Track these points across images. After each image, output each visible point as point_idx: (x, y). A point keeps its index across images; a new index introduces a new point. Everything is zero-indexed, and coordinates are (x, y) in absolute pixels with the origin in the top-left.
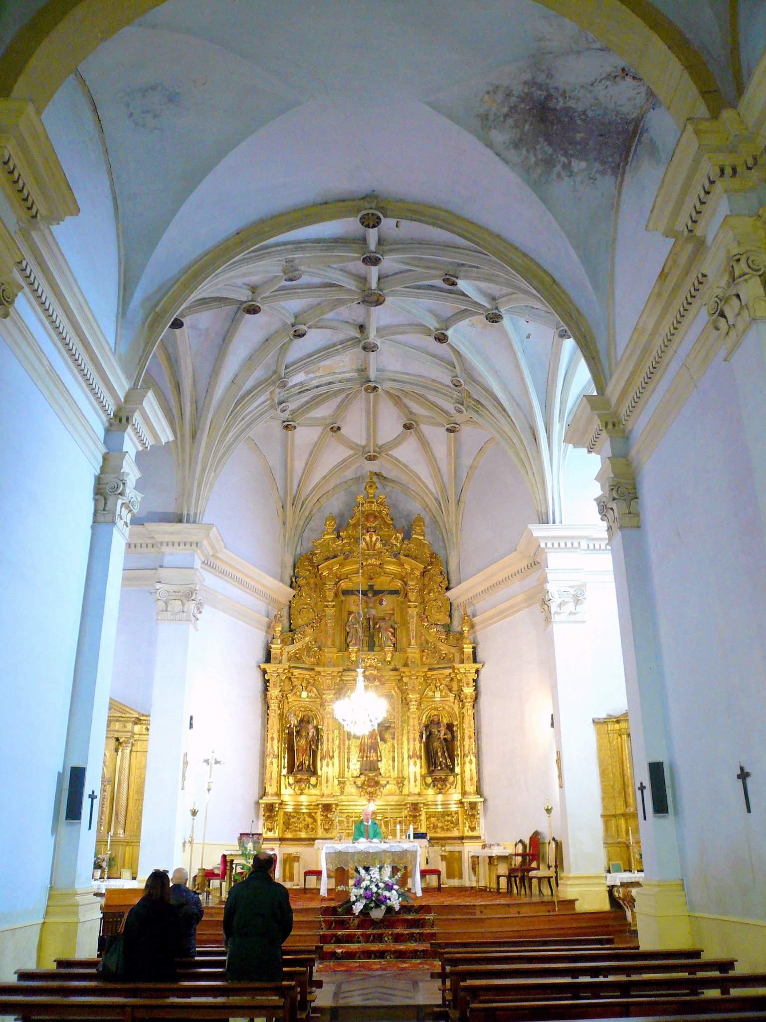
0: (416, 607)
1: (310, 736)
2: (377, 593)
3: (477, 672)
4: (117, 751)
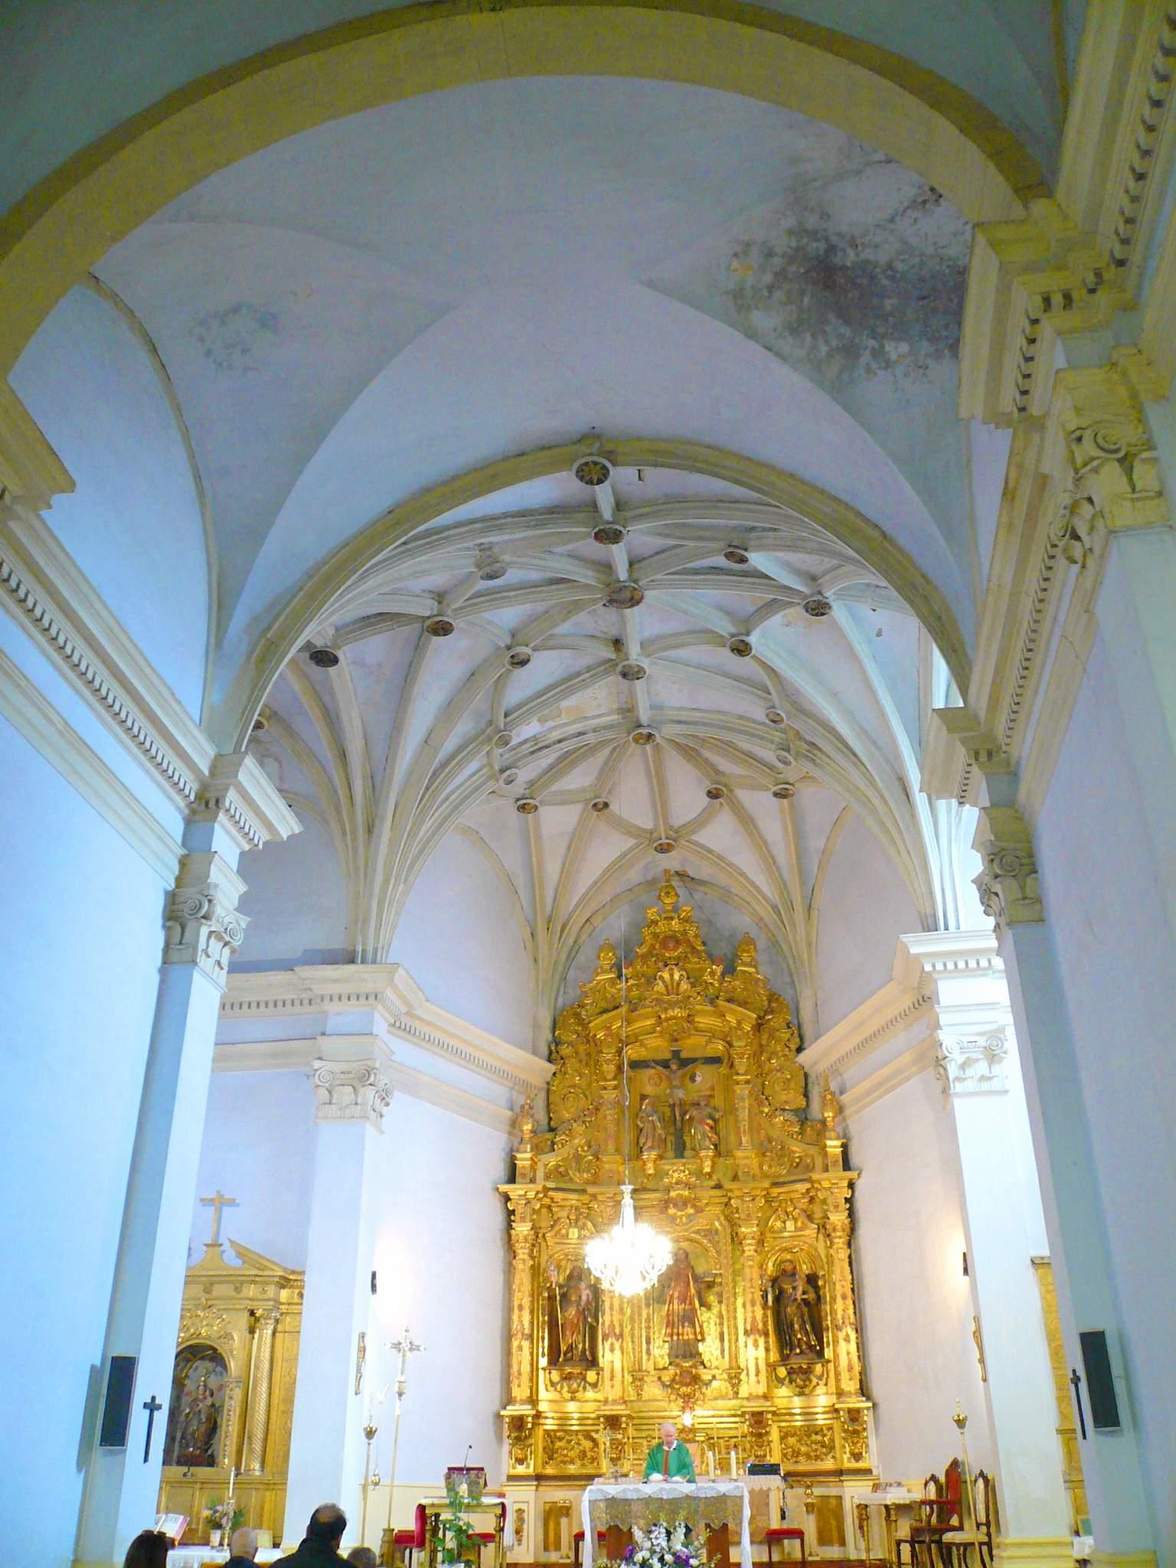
0: (747, 1082)
2: (685, 1063)
3: (851, 1185)
4: (252, 1331)
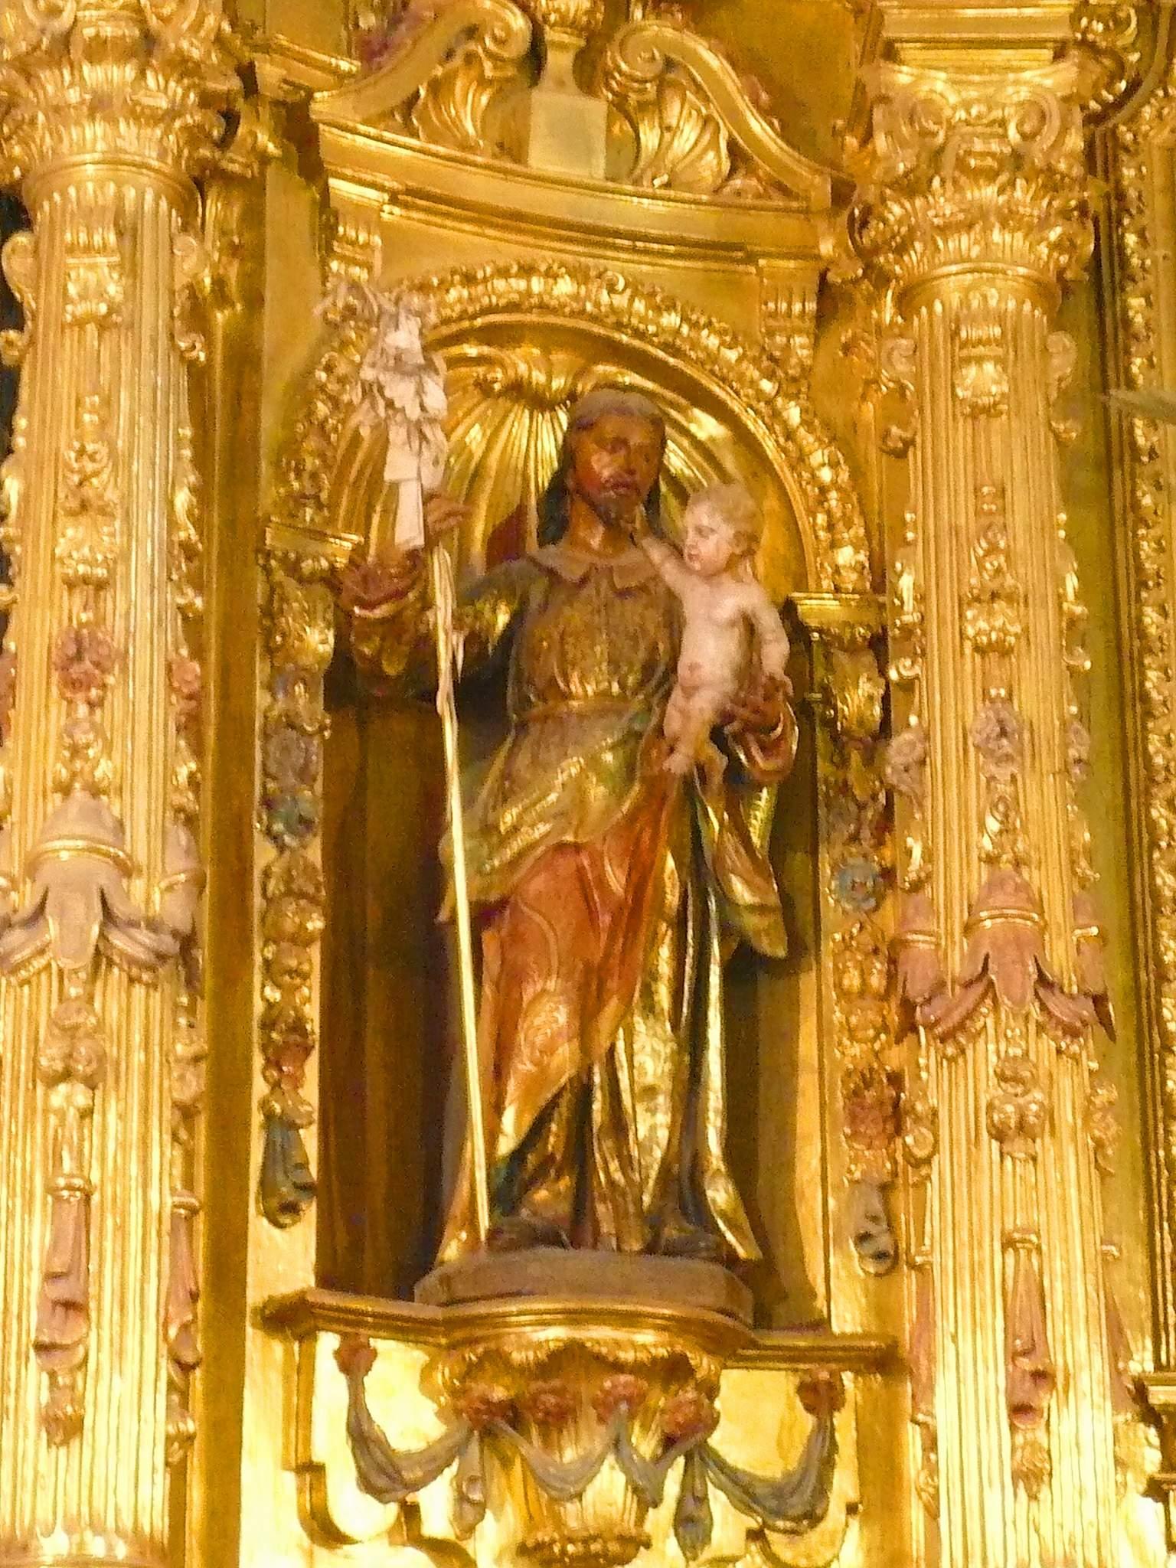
1: (693, 711)
